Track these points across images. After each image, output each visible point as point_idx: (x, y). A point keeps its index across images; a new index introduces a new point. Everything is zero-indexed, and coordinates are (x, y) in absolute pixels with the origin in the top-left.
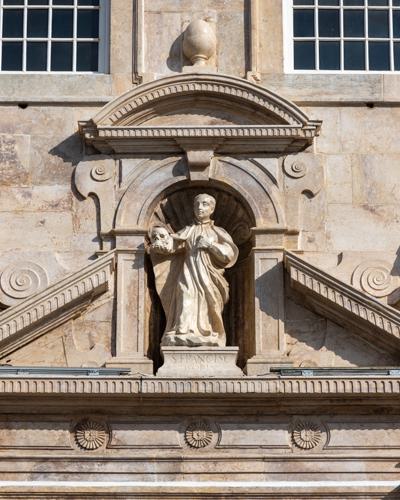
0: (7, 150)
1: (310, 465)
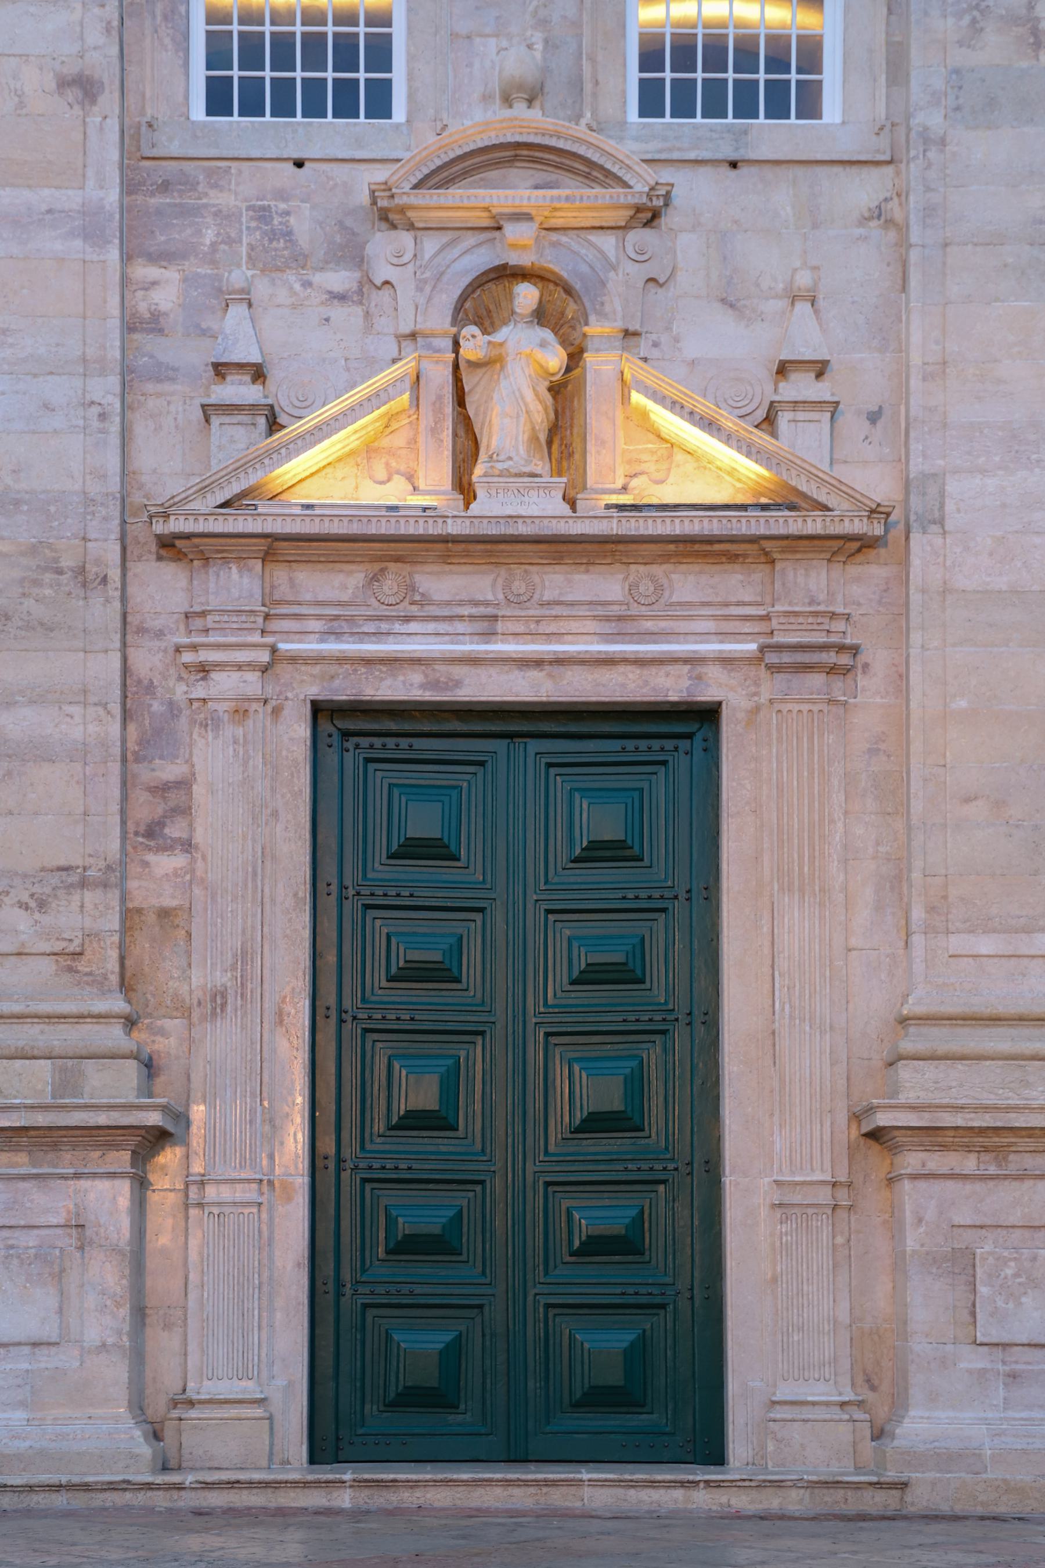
0: (281, 223)
1: (649, 625)
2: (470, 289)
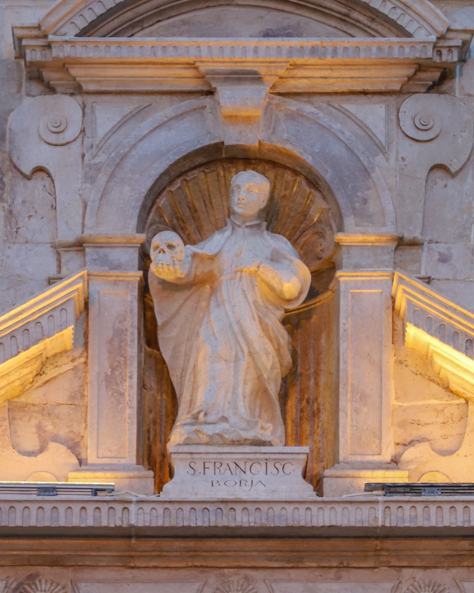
2: (166, 179)
